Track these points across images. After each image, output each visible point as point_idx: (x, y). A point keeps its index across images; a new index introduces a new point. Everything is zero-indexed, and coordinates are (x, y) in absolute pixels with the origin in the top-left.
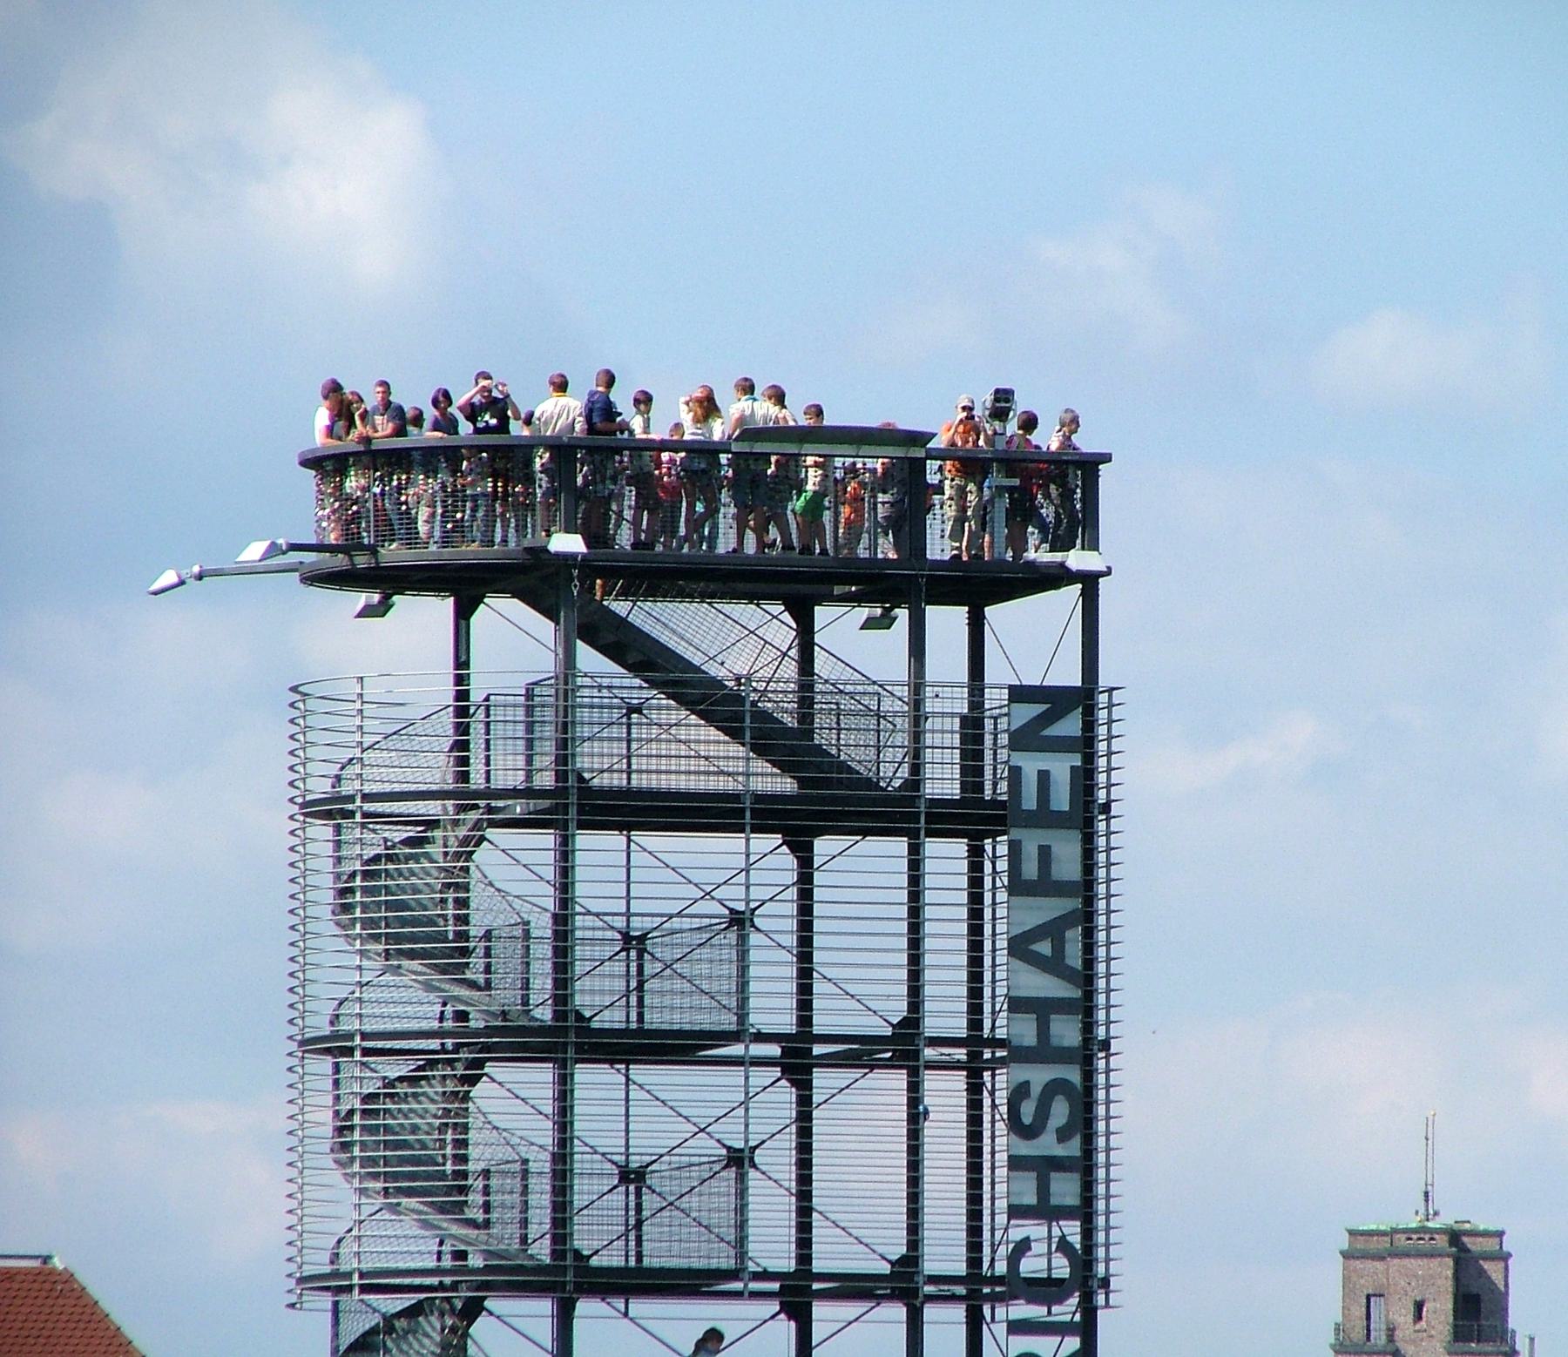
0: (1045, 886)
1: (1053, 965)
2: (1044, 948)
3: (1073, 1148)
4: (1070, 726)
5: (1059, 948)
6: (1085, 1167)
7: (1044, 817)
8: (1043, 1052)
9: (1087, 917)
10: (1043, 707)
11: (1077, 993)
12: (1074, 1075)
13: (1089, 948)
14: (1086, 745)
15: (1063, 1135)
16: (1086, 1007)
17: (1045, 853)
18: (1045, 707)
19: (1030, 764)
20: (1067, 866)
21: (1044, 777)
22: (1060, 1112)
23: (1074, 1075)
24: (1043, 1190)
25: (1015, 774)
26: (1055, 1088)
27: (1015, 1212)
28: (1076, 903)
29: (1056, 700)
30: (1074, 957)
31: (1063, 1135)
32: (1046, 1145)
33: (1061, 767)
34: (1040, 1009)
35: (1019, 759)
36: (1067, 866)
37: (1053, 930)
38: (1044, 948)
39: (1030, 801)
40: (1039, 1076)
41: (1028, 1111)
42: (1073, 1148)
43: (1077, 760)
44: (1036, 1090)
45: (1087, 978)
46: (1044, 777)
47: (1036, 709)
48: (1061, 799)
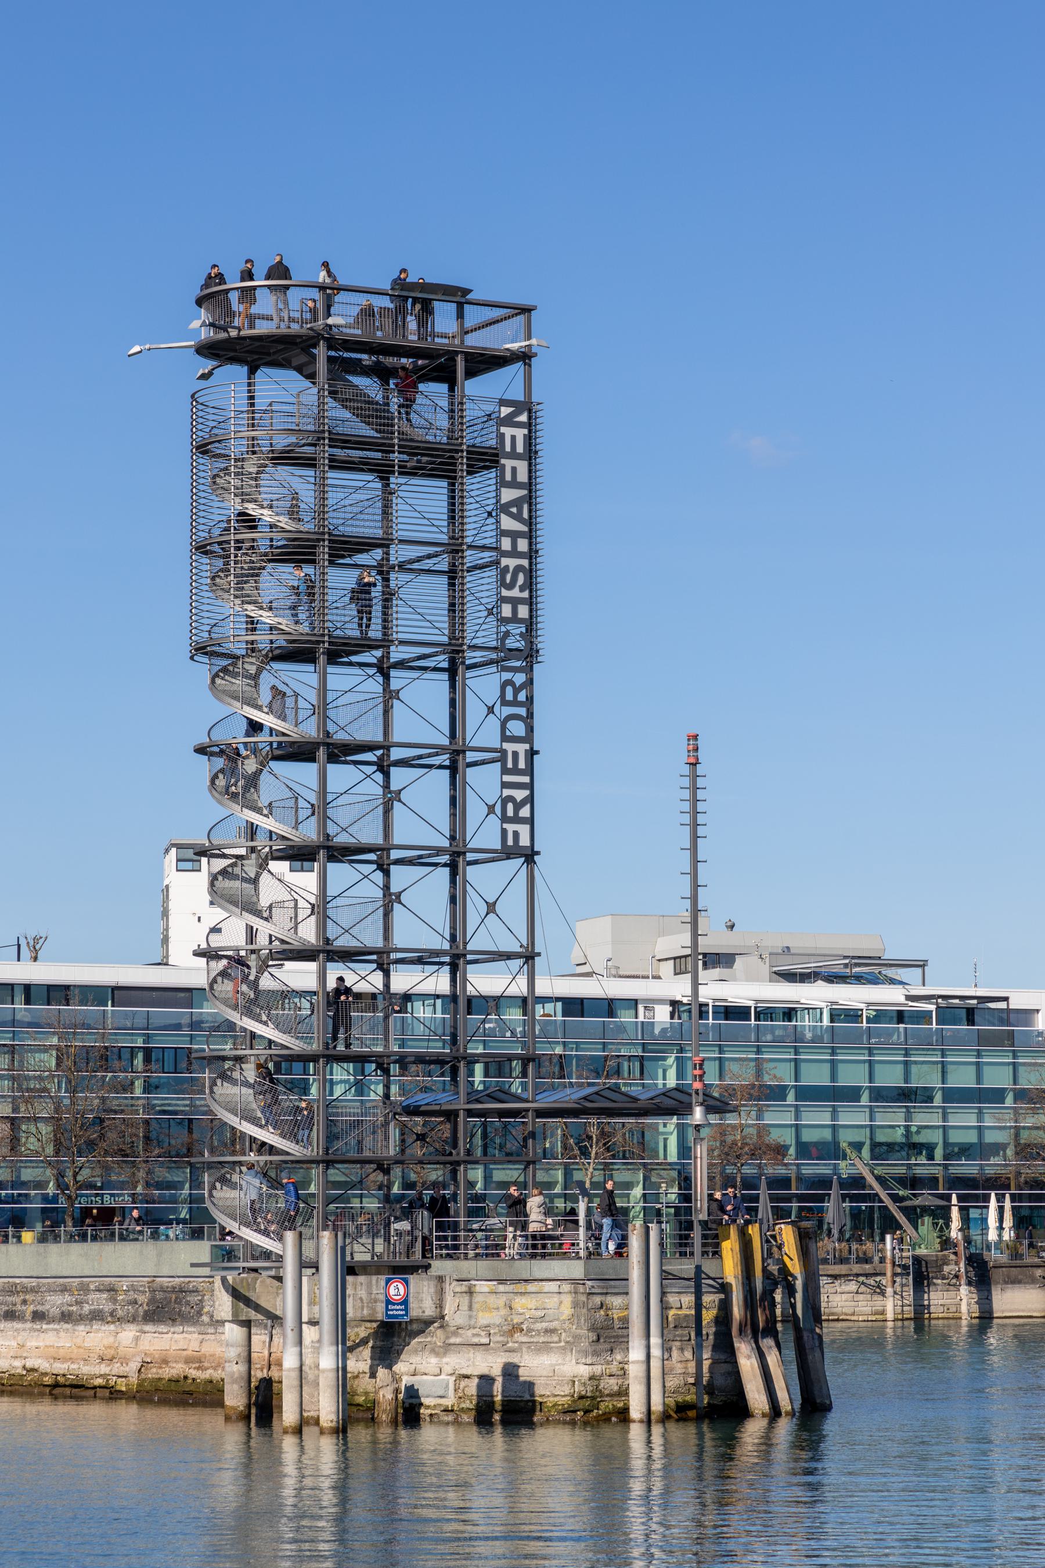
0: (514, 484)
1: (518, 517)
2: (514, 510)
4: (523, 418)
5: (520, 511)
7: (514, 455)
8: (514, 553)
9: (530, 499)
10: (512, 409)
11: (525, 529)
14: (529, 425)
15: (522, 590)
16: (531, 536)
17: (514, 470)
18: (512, 409)
19: (508, 431)
21: (513, 438)
22: (521, 579)
23: (525, 563)
25: (501, 437)
26: (518, 569)
28: (525, 492)
29: (519, 406)
30: (526, 515)
31: (522, 590)
32: (515, 593)
33: (520, 433)
34: (514, 535)
35: (503, 429)
36: (523, 477)
37: (517, 502)
38: (514, 510)
39: (508, 449)
40: (511, 563)
42: (526, 594)
43: (526, 431)
44: (511, 569)
45: (531, 523)
46: (513, 438)
47: (510, 410)
48: (520, 449)
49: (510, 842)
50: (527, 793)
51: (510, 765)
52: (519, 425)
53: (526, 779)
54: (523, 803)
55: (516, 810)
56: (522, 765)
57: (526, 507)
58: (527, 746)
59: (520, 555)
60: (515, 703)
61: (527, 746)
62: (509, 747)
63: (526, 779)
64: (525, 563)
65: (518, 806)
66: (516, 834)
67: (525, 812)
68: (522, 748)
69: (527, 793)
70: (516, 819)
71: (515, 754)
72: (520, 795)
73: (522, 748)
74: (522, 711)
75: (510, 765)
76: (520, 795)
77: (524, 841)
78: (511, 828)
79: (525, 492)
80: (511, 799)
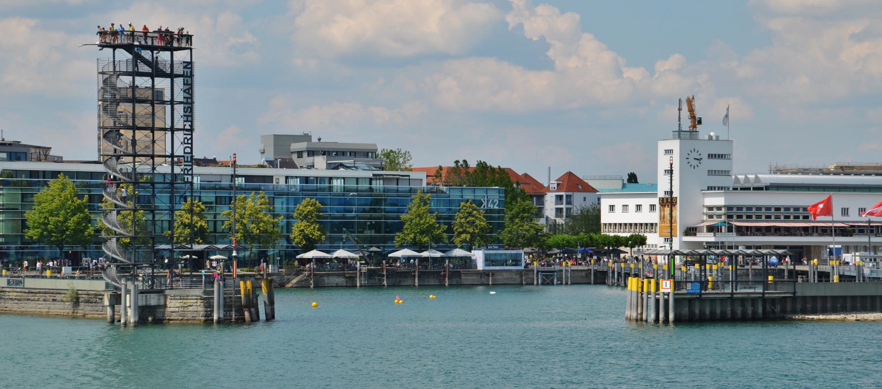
1: (188, 93)
2: (187, 91)
3: (190, 114)
4: (190, 66)
5: (189, 91)
6: (192, 116)
11: (190, 96)
12: (190, 106)
13: (192, 91)
15: (189, 113)
16: (191, 98)
20: (189, 82)
21: (187, 72)
22: (189, 110)
24: (187, 119)
26: (189, 107)
27: (184, 121)
28: (190, 86)
32: (188, 114)
33: (189, 70)
37: (188, 89)
38: (187, 91)
40: (187, 106)
41: (186, 110)
45: (192, 95)
46: (187, 72)
48: (189, 75)
49: (186, 180)
50: (191, 167)
51: (186, 160)
52: (189, 68)
53: (191, 164)
54: (190, 170)
55: (188, 172)
56: (189, 160)
57: (190, 90)
58: (191, 155)
59: (189, 104)
60: (188, 143)
61: (191, 155)
62: (186, 155)
63: (191, 164)
64: (190, 106)
66: (187, 178)
69: (191, 167)
70: (188, 174)
71: (187, 157)
74: (190, 146)
75: (186, 160)
76: (189, 168)
77: (190, 180)
78: (186, 177)
79: (190, 86)
80: (186, 169)
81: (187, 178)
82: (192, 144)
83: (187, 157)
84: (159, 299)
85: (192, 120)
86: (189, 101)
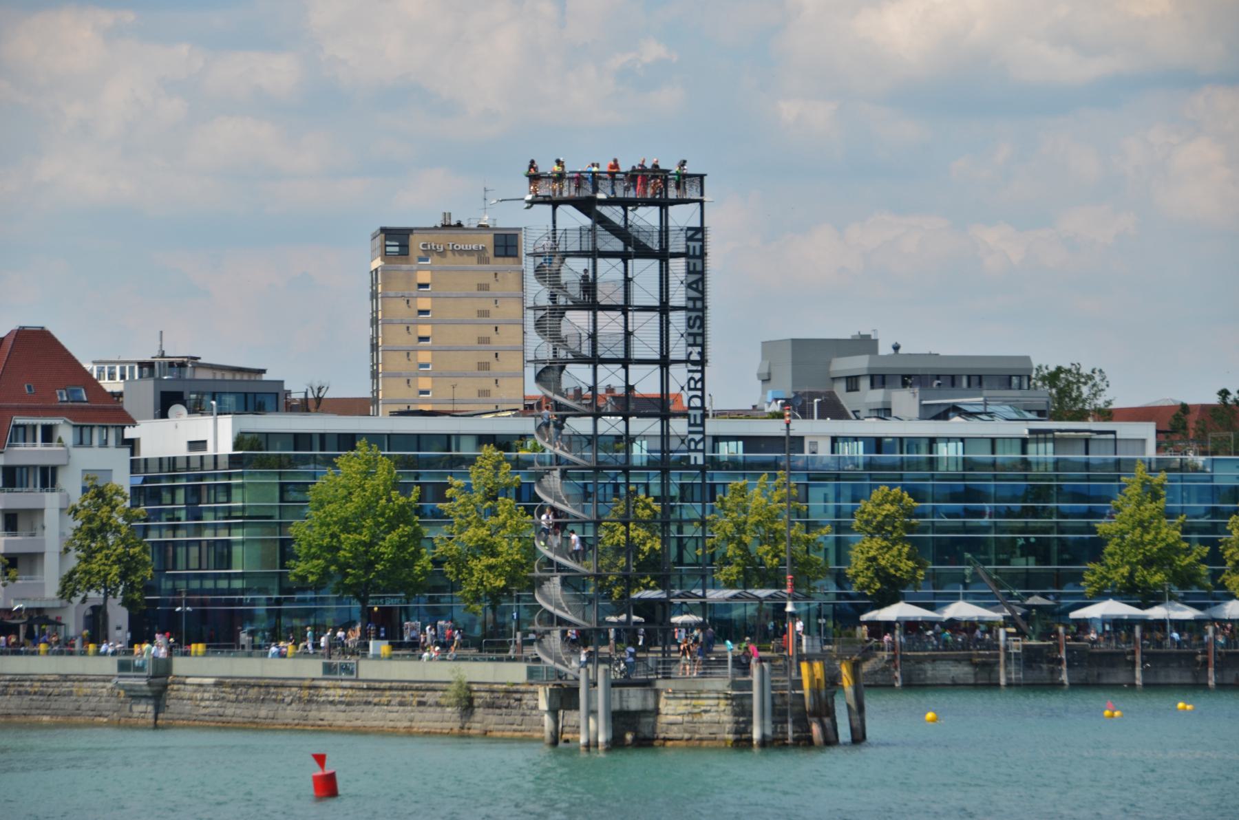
1: (696, 290)
2: (694, 286)
3: (700, 331)
4: (699, 236)
13: (703, 285)
15: (699, 328)
16: (703, 299)
21: (694, 247)
22: (698, 323)
26: (697, 317)
30: (700, 288)
31: (699, 328)
32: (695, 330)
33: (698, 245)
37: (696, 282)
38: (694, 286)
41: (691, 322)
46: (694, 247)
48: (698, 253)
51: (692, 422)
54: (700, 441)
56: (699, 421)
58: (701, 412)
59: (698, 310)
61: (701, 412)
63: (700, 429)
65: (697, 443)
66: (696, 458)
67: (700, 446)
68: (699, 412)
70: (696, 450)
71: (695, 416)
72: (698, 437)
73: (699, 412)
74: (699, 393)
75: (692, 422)
76: (698, 437)
78: (693, 455)
80: (693, 440)
81: (696, 458)
82: (702, 389)
83: (695, 416)
84: (645, 699)
85: (704, 341)
86: (699, 304)
